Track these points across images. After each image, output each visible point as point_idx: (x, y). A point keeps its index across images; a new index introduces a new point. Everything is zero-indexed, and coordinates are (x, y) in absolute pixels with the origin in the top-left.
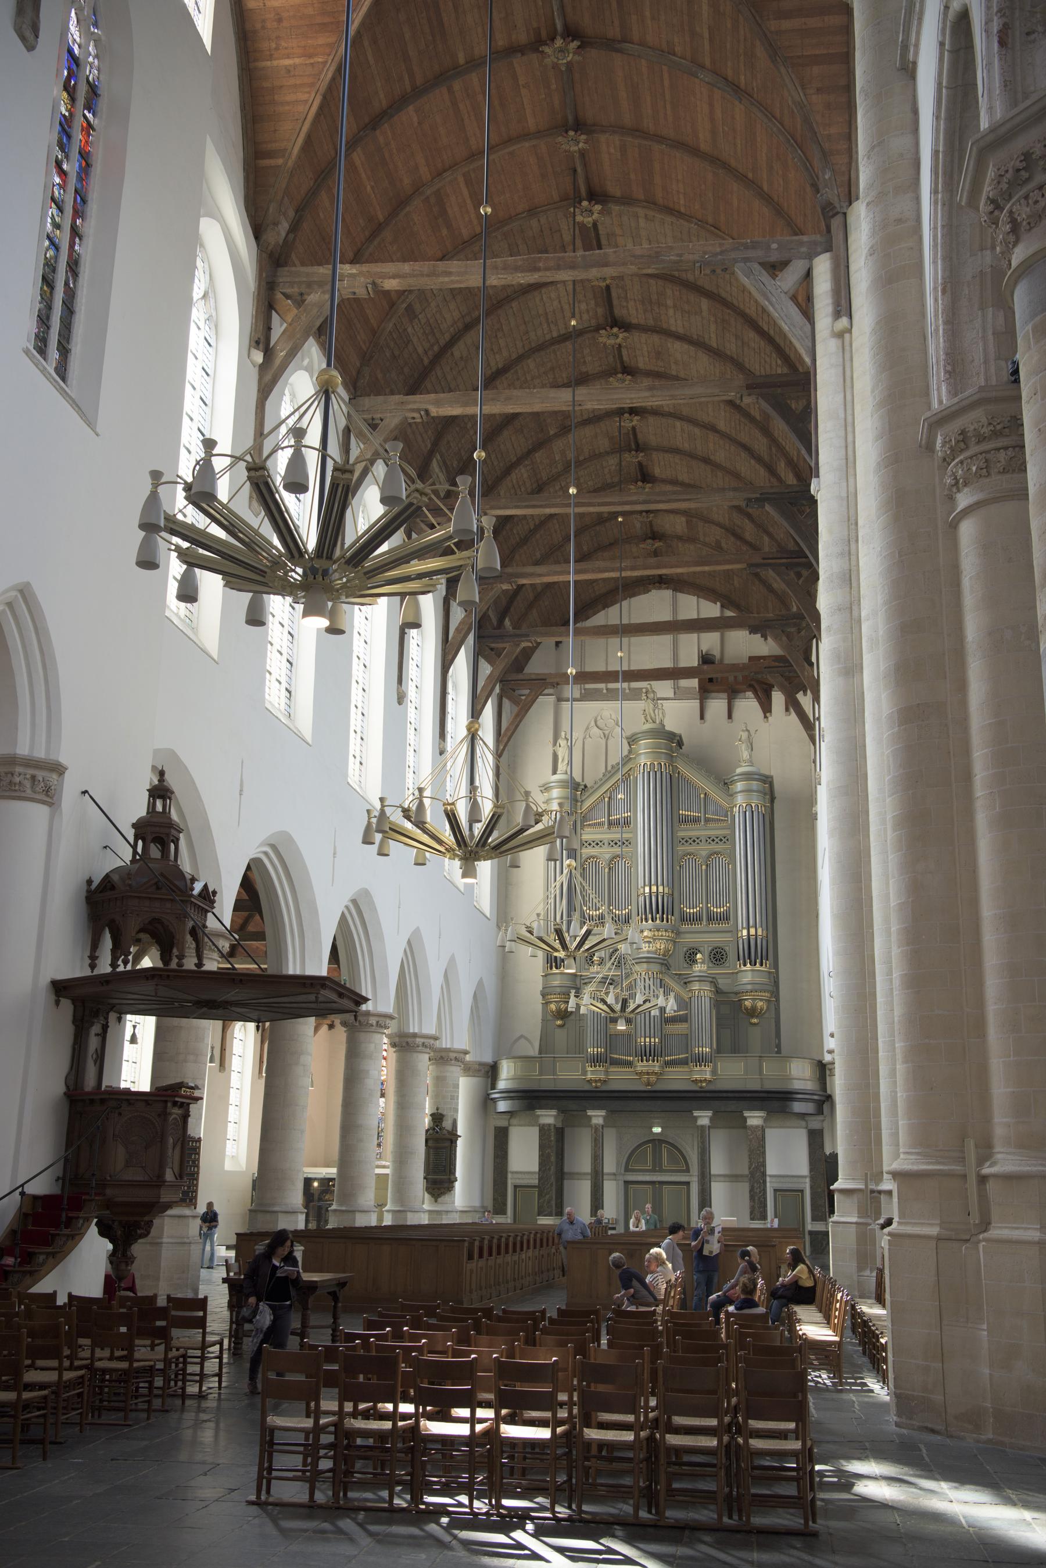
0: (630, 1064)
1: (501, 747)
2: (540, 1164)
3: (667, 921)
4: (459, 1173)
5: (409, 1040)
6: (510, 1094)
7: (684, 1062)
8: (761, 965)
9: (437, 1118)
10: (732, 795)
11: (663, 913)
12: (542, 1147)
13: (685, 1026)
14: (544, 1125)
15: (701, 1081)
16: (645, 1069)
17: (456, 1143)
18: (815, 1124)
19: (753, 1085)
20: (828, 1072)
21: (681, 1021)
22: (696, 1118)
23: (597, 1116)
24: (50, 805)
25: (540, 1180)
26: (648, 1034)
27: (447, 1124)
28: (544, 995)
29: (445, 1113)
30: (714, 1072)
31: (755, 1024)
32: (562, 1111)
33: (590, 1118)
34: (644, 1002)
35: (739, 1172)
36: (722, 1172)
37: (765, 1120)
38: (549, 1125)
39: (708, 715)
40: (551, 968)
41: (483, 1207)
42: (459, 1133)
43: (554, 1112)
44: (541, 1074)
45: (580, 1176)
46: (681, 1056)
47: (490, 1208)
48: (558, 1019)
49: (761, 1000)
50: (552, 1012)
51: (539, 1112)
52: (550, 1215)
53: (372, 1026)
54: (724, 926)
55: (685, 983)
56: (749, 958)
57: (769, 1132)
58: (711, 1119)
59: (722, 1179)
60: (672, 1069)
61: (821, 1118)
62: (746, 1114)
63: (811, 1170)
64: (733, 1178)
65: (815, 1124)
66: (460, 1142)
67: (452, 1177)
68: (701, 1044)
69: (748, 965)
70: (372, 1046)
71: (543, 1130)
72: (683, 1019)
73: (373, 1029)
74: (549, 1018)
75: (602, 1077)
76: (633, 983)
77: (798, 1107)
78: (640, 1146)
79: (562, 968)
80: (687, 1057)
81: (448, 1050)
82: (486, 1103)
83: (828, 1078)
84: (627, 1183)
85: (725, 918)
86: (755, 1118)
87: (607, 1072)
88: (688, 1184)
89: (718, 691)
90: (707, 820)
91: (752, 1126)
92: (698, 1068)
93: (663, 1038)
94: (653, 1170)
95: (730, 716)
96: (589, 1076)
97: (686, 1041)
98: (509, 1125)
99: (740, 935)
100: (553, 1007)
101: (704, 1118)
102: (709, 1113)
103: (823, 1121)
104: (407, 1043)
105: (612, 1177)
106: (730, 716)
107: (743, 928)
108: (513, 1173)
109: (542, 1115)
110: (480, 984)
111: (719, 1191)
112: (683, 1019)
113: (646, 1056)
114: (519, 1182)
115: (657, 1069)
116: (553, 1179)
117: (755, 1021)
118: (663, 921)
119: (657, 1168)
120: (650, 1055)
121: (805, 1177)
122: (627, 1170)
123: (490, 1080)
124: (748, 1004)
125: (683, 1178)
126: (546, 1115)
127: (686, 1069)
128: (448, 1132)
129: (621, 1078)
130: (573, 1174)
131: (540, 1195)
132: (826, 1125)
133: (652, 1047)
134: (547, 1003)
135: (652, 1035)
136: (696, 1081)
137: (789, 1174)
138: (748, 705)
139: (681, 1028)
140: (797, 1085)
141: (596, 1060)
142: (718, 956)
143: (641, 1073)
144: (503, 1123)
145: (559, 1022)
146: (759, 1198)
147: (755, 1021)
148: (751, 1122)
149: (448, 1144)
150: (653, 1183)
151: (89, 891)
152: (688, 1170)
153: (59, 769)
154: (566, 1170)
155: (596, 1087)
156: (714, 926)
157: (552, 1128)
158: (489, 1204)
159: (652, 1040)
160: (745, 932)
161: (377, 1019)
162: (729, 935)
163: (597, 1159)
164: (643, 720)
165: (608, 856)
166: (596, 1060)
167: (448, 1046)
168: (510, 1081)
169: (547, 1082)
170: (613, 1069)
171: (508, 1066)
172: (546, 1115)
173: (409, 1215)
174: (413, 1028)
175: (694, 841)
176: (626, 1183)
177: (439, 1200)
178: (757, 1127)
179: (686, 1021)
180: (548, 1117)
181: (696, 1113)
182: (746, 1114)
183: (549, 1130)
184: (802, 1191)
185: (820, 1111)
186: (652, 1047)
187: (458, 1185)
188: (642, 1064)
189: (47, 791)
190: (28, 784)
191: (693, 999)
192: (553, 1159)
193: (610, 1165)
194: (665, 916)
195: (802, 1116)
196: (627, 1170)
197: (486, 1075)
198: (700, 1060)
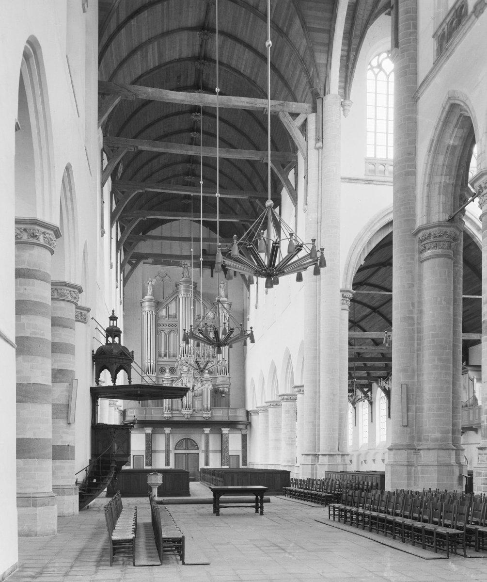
18: (244, 432)
19: (226, 419)
22: (204, 431)
23: (167, 430)
24: (85, 323)
30: (211, 414)
35: (217, 449)
36: (214, 449)
37: (229, 431)
43: (151, 429)
51: (146, 429)
56: (222, 372)
57: (230, 436)
58: (210, 431)
61: (246, 430)
62: (223, 429)
65: (244, 432)
75: (170, 416)
77: (240, 426)
78: (179, 441)
83: (249, 416)
84: (175, 454)
86: (225, 430)
88: (198, 454)
95: (212, 276)
96: (165, 415)
101: (207, 430)
106: (212, 276)
111: (211, 456)
117: (224, 395)
119: (187, 448)
122: (175, 449)
124: (221, 389)
132: (248, 433)
139: (199, 398)
141: (167, 410)
147: (224, 395)
148: (223, 432)
151: (93, 354)
153: (88, 310)
163: (168, 445)
164: (182, 276)
166: (167, 410)
176: (175, 454)
182: (223, 429)
189: (85, 319)
190: (80, 316)
195: (241, 429)
198: (206, 410)
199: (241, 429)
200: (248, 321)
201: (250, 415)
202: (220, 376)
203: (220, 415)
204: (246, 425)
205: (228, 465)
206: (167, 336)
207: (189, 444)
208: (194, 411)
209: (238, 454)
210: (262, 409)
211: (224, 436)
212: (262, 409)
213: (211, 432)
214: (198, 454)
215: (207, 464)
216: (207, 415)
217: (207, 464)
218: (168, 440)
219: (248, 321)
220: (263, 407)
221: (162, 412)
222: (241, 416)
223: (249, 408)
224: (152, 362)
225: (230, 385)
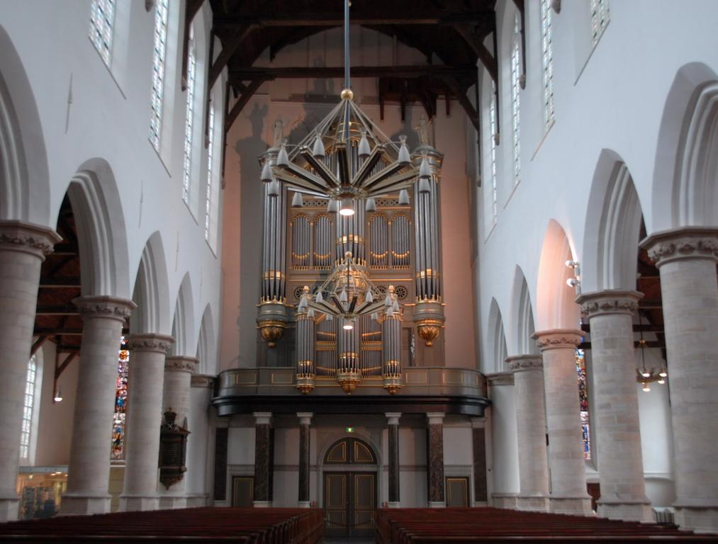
0: (334, 375)
1: (229, 124)
2: (256, 458)
3: (361, 264)
4: (187, 464)
5: (147, 340)
6: (230, 400)
7: (379, 373)
8: (436, 299)
9: (169, 416)
11: (357, 257)
12: (258, 443)
13: (379, 343)
14: (260, 425)
15: (392, 388)
16: (345, 378)
17: (186, 438)
18: (478, 424)
20: (488, 383)
21: (375, 340)
22: (387, 419)
23: (306, 418)
25: (255, 471)
26: (349, 350)
27: (179, 422)
28: (258, 322)
29: (177, 412)
30: (403, 381)
31: (430, 346)
32: (275, 415)
33: (299, 419)
34: (375, 300)
37: (444, 419)
38: (265, 425)
39: (385, 117)
40: (266, 300)
41: (205, 494)
42: (189, 429)
43: (269, 414)
44: (258, 383)
45: (290, 467)
47: (211, 494)
48: (270, 341)
49: (435, 326)
50: (266, 335)
51: (256, 414)
52: (264, 499)
53: (110, 312)
54: (405, 269)
56: (426, 293)
57: (444, 430)
58: (400, 420)
61: (483, 419)
62: (429, 415)
63: (475, 461)
64: (416, 468)
66: (189, 438)
67: (183, 467)
68: (393, 358)
69: (426, 299)
70: (110, 332)
71: (260, 430)
72: (378, 338)
73: (111, 315)
74: (263, 340)
77: (468, 409)
79: (275, 300)
81: (181, 359)
82: (211, 408)
83: (488, 388)
84: (325, 473)
85: (406, 262)
87: (314, 381)
88: (375, 474)
89: (395, 100)
91: (433, 425)
92: (388, 378)
94: (348, 463)
95: (403, 118)
97: (382, 356)
98: (229, 426)
99: (418, 275)
100: (266, 331)
101: (394, 418)
102: (399, 415)
103: (484, 421)
105: (315, 469)
108: (231, 466)
109: (259, 417)
110: (208, 309)
111: (405, 479)
112: (378, 338)
113: (347, 367)
114: (236, 473)
115: (356, 379)
116: (267, 469)
117: (430, 343)
118: (357, 263)
120: (351, 367)
121: (470, 466)
123: (213, 391)
127: (380, 378)
128: (180, 428)
129: (325, 386)
130: (284, 466)
131: (255, 484)
132: (487, 426)
133: (353, 361)
134: (261, 329)
135: (353, 351)
136: (388, 389)
137: (457, 464)
138: (418, 111)
139: (376, 345)
140: (466, 392)
142: (401, 293)
143: (342, 383)
144: (222, 425)
145: (271, 344)
146: (439, 484)
147: (430, 343)
149: (179, 439)
150: (346, 473)
152: (375, 460)
154: (276, 462)
155: (305, 393)
156: (398, 269)
157: (267, 427)
158: (210, 490)
159: (353, 354)
160: (423, 274)
161: (116, 305)
162: (409, 276)
163: (303, 452)
165: (312, 213)
167: (181, 355)
168: (231, 390)
169: (264, 390)
170: (319, 378)
171: (229, 377)
173: (144, 502)
174: (151, 330)
175: (382, 203)
177: (172, 487)
178: (437, 425)
179: (380, 340)
180: (263, 418)
181: (388, 415)
183: (264, 429)
184: (468, 478)
185: (482, 415)
186: (353, 361)
187: (186, 474)
188: (344, 374)
192: (267, 453)
193: (313, 459)
194: (359, 259)
196: (325, 462)
197: (210, 386)
198: (393, 371)
199: (470, 417)
200: (478, 188)
201: (491, 385)
202: (421, 301)
203: (419, 382)
204: (483, 407)
205: (442, 500)
206: (312, 224)
207: (356, 447)
208: (364, 374)
209: (466, 474)
210: (521, 362)
211: (431, 430)
212: (521, 362)
213: (403, 422)
215: (394, 496)
216: (394, 382)
217: (394, 496)
218: (304, 440)
219: (478, 188)
220: (524, 357)
221: (295, 377)
222: (469, 386)
223: (488, 369)
224: (278, 275)
225: (443, 320)
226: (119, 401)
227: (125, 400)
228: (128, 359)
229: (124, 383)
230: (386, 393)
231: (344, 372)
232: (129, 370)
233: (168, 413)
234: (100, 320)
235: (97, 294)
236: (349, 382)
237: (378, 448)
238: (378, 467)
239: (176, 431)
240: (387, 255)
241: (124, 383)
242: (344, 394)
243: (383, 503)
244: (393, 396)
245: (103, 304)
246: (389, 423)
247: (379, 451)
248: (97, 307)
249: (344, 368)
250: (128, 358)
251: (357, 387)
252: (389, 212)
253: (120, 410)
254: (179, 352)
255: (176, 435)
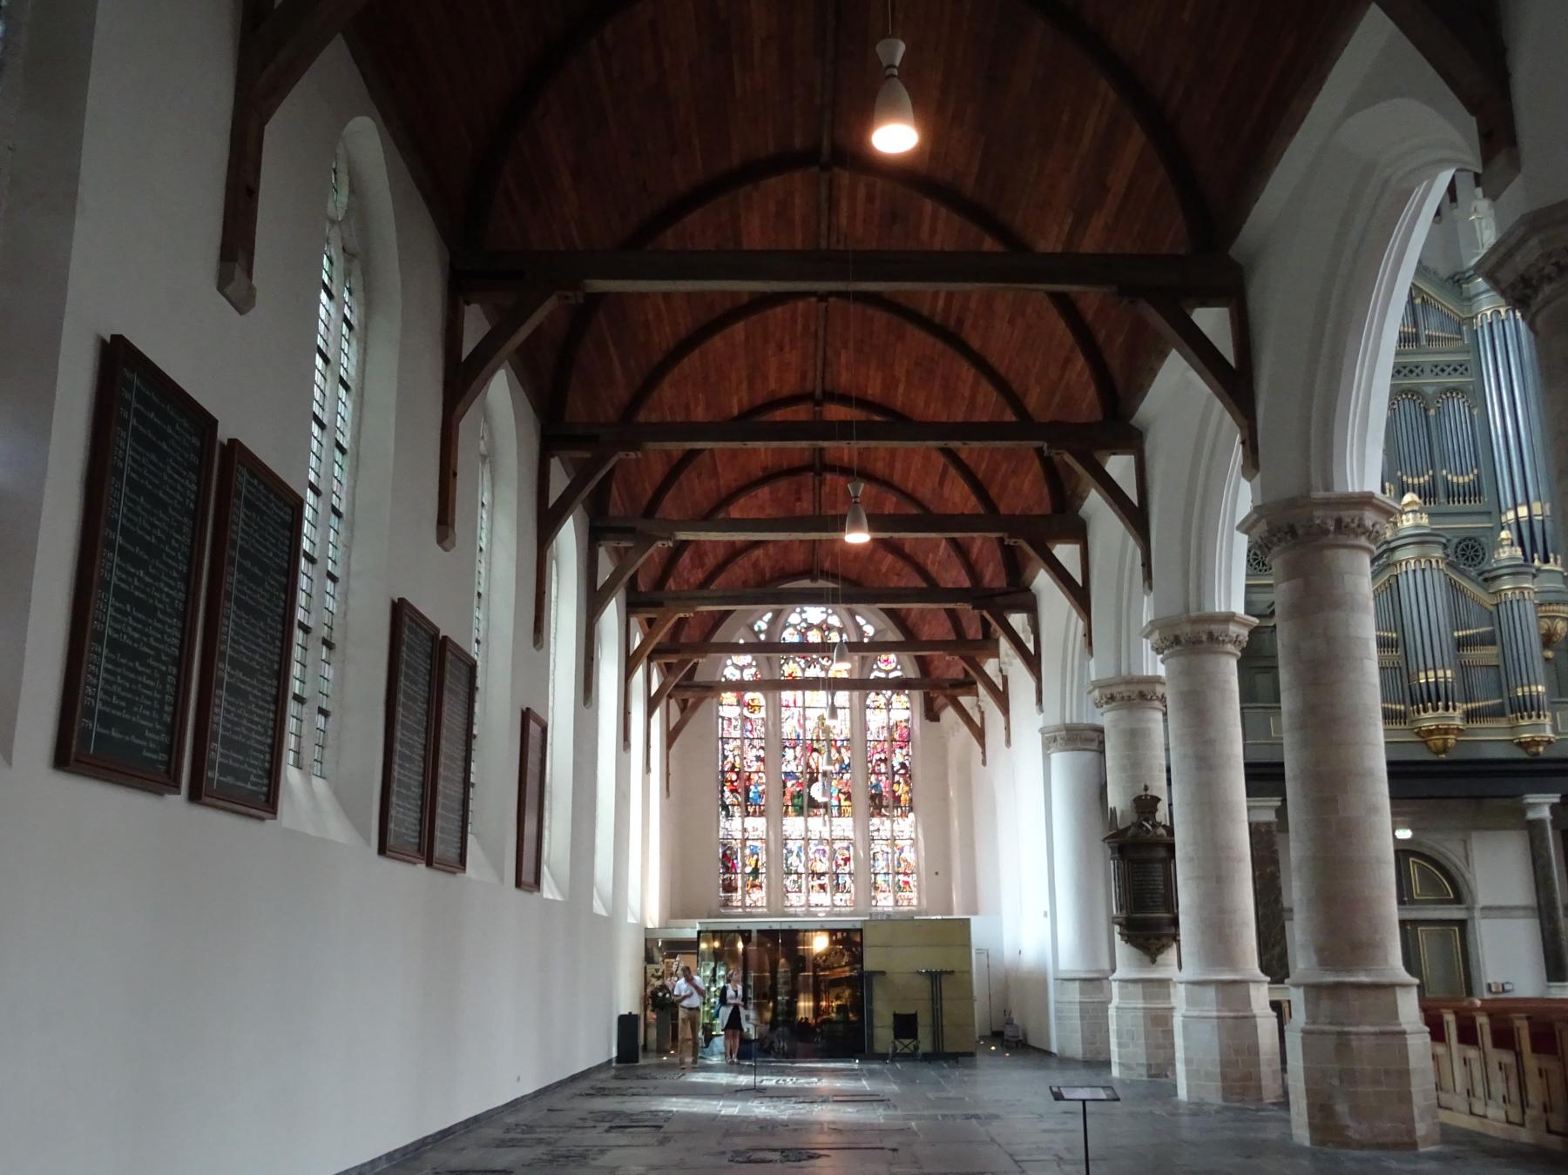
5: (1215, 628)
7: (1498, 712)
10: (1469, 299)
16: (1431, 725)
21: (1483, 644)
22: (1522, 811)
38: (1268, 824)
46: (1490, 702)
54: (1474, 506)
55: (1486, 580)
59: (1521, 913)
60: (1478, 725)
68: (1525, 681)
72: (1488, 640)
76: (1393, 581)
80: (1502, 704)
85: (1473, 491)
88: (1462, 924)
90: (1429, 339)
92: (1525, 722)
93: (1464, 669)
97: (1502, 676)
104: (1211, 635)
107: (1508, 509)
125: (1455, 913)
126: (1261, 807)
127: (1503, 723)
136: (1522, 745)
139: (1485, 655)
149: (1162, 853)
167: (1150, 673)
172: (1261, 807)
177: (1160, 958)
179: (1493, 643)
191: (1502, 608)
208: (1470, 716)
214: (1462, 924)
226: (751, 795)
227: (763, 792)
228: (763, 714)
229: (759, 758)
230: (1520, 754)
231: (1425, 710)
232: (766, 732)
233: (1140, 797)
234: (1343, 553)
235: (1338, 489)
236: (1447, 731)
237: (1464, 870)
238: (1470, 909)
239: (1162, 835)
240: (1433, 477)
241: (759, 758)
242: (1431, 757)
243: (1489, 986)
244: (1536, 760)
245: (1355, 513)
246: (1531, 815)
247: (1468, 876)
248: (1339, 522)
249: (1423, 703)
250: (763, 709)
251: (1457, 741)
252: (1430, 390)
253: (755, 812)
254: (1147, 669)
255: (1156, 843)
